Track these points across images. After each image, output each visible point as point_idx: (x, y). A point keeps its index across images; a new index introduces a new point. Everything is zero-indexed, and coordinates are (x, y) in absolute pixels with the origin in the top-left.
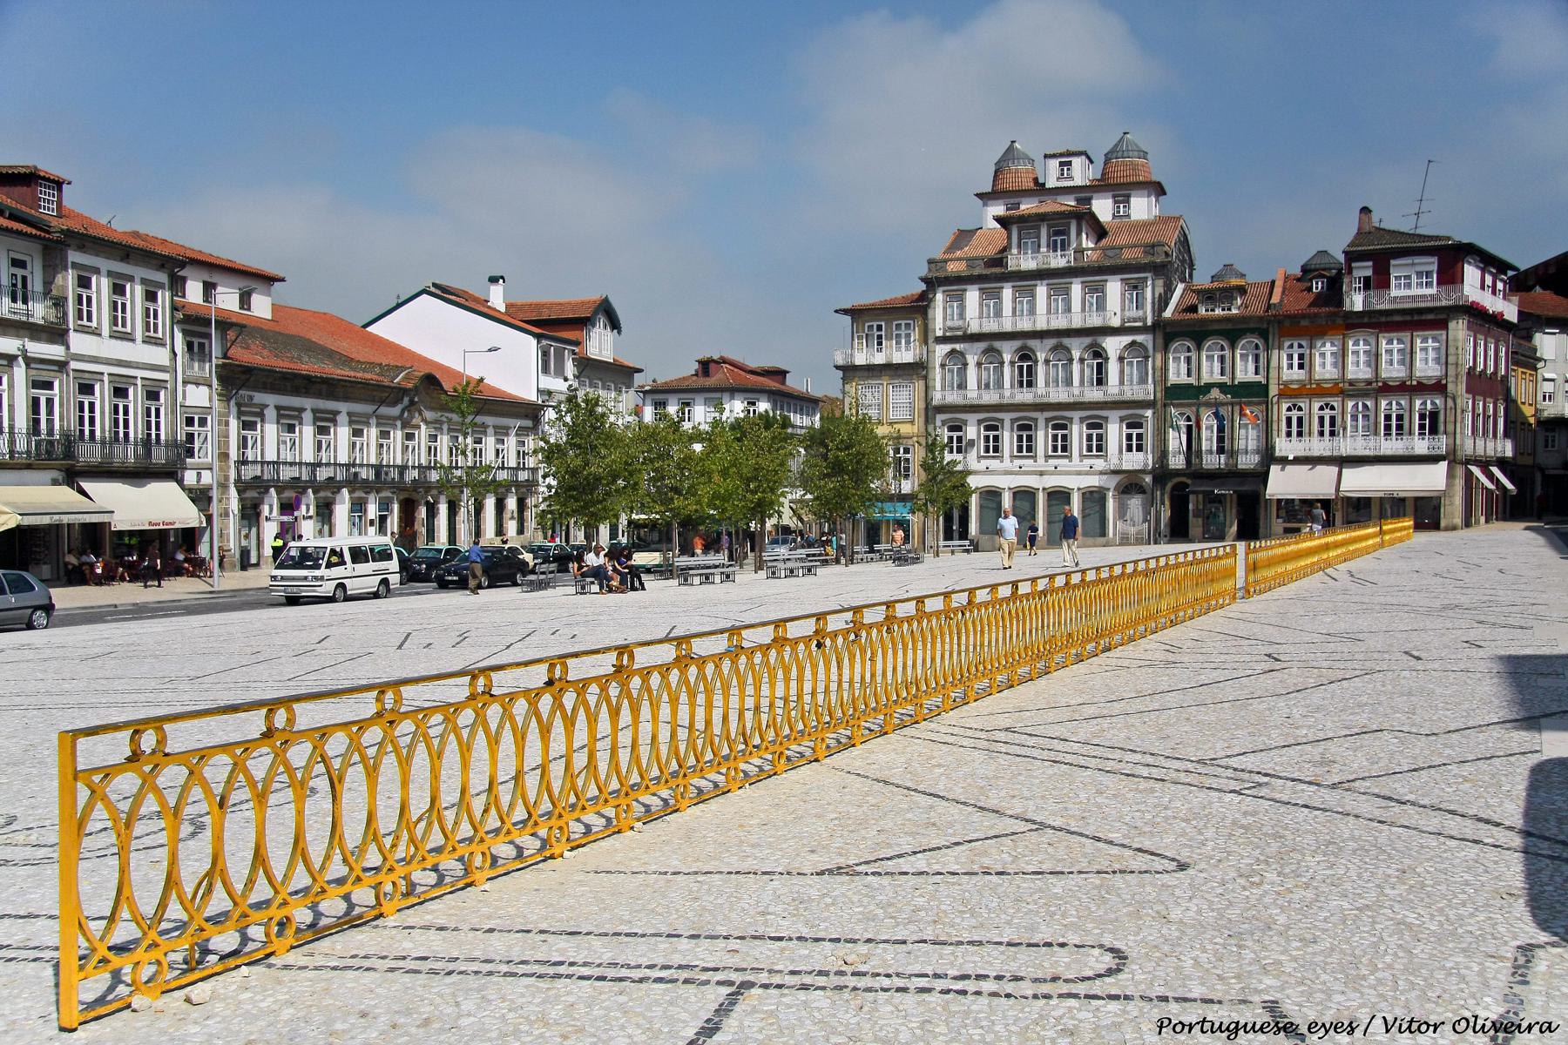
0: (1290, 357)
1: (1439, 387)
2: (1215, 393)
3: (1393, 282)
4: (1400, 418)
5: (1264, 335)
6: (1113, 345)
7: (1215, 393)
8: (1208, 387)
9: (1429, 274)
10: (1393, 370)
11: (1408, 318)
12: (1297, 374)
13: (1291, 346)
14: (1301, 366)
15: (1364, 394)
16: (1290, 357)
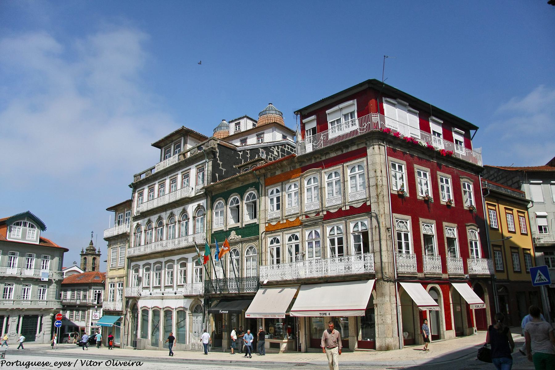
0: (272, 200)
1: (365, 209)
2: (233, 236)
3: (330, 126)
4: (340, 241)
5: (256, 186)
6: (191, 208)
7: (233, 236)
8: (231, 229)
9: (352, 114)
10: (333, 201)
11: (339, 153)
12: (276, 214)
13: (272, 193)
14: (278, 208)
15: (314, 223)
16: (272, 200)
